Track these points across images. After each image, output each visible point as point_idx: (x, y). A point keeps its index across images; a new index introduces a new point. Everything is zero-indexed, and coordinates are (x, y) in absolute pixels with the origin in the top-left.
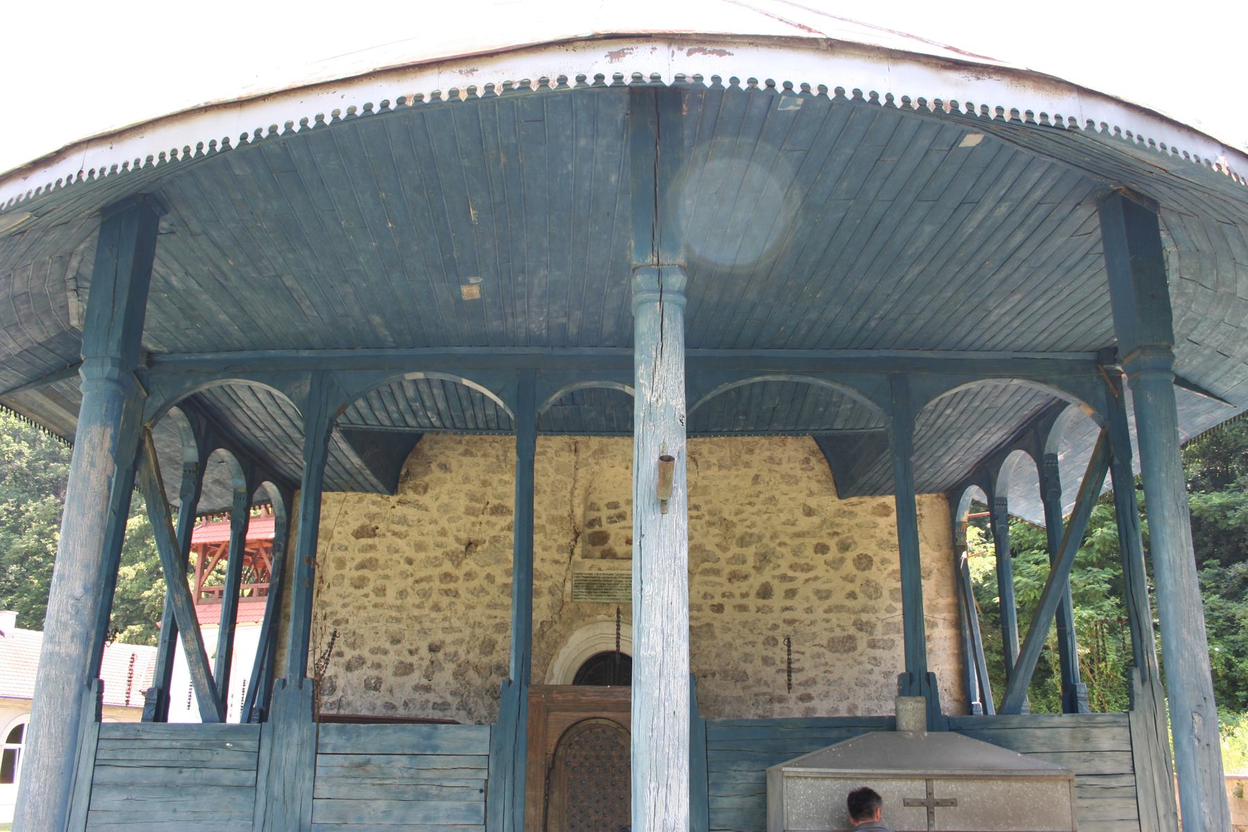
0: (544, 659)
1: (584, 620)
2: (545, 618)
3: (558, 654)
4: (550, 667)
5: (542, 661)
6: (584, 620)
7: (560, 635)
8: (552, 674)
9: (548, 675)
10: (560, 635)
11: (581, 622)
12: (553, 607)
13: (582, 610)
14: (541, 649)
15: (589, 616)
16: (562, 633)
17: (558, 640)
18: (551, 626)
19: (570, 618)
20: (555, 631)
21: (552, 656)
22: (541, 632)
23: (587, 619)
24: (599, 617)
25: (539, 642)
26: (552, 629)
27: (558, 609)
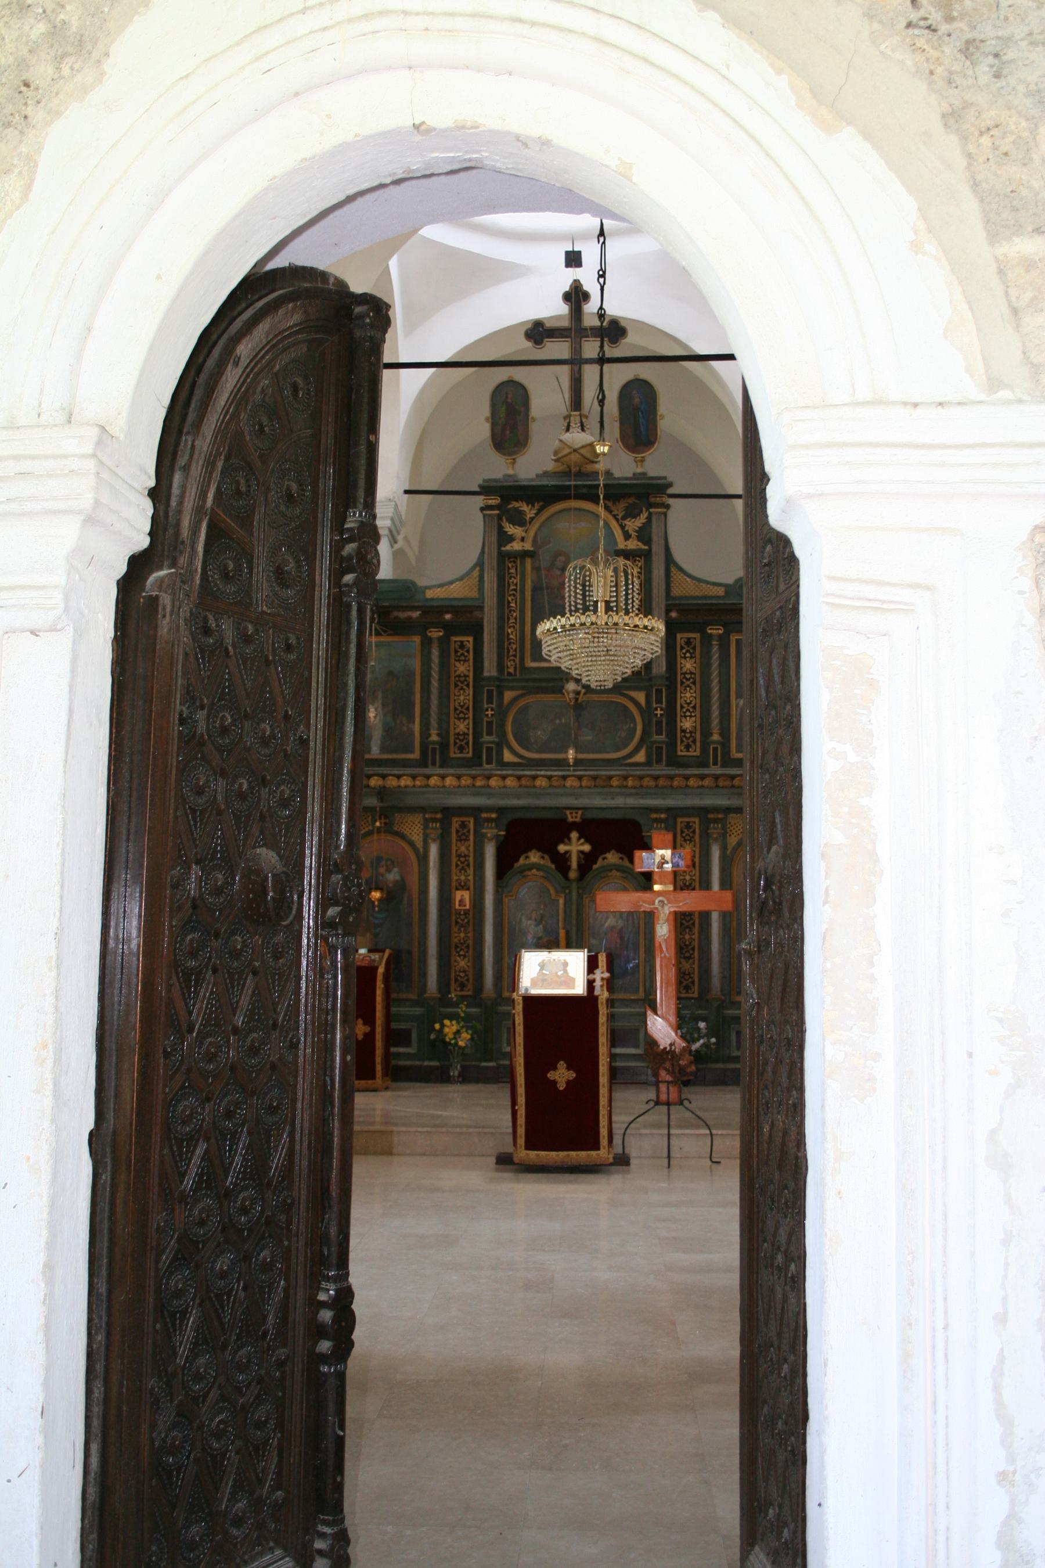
7: (57, 31)
10: (57, 31)
17: (41, 71)
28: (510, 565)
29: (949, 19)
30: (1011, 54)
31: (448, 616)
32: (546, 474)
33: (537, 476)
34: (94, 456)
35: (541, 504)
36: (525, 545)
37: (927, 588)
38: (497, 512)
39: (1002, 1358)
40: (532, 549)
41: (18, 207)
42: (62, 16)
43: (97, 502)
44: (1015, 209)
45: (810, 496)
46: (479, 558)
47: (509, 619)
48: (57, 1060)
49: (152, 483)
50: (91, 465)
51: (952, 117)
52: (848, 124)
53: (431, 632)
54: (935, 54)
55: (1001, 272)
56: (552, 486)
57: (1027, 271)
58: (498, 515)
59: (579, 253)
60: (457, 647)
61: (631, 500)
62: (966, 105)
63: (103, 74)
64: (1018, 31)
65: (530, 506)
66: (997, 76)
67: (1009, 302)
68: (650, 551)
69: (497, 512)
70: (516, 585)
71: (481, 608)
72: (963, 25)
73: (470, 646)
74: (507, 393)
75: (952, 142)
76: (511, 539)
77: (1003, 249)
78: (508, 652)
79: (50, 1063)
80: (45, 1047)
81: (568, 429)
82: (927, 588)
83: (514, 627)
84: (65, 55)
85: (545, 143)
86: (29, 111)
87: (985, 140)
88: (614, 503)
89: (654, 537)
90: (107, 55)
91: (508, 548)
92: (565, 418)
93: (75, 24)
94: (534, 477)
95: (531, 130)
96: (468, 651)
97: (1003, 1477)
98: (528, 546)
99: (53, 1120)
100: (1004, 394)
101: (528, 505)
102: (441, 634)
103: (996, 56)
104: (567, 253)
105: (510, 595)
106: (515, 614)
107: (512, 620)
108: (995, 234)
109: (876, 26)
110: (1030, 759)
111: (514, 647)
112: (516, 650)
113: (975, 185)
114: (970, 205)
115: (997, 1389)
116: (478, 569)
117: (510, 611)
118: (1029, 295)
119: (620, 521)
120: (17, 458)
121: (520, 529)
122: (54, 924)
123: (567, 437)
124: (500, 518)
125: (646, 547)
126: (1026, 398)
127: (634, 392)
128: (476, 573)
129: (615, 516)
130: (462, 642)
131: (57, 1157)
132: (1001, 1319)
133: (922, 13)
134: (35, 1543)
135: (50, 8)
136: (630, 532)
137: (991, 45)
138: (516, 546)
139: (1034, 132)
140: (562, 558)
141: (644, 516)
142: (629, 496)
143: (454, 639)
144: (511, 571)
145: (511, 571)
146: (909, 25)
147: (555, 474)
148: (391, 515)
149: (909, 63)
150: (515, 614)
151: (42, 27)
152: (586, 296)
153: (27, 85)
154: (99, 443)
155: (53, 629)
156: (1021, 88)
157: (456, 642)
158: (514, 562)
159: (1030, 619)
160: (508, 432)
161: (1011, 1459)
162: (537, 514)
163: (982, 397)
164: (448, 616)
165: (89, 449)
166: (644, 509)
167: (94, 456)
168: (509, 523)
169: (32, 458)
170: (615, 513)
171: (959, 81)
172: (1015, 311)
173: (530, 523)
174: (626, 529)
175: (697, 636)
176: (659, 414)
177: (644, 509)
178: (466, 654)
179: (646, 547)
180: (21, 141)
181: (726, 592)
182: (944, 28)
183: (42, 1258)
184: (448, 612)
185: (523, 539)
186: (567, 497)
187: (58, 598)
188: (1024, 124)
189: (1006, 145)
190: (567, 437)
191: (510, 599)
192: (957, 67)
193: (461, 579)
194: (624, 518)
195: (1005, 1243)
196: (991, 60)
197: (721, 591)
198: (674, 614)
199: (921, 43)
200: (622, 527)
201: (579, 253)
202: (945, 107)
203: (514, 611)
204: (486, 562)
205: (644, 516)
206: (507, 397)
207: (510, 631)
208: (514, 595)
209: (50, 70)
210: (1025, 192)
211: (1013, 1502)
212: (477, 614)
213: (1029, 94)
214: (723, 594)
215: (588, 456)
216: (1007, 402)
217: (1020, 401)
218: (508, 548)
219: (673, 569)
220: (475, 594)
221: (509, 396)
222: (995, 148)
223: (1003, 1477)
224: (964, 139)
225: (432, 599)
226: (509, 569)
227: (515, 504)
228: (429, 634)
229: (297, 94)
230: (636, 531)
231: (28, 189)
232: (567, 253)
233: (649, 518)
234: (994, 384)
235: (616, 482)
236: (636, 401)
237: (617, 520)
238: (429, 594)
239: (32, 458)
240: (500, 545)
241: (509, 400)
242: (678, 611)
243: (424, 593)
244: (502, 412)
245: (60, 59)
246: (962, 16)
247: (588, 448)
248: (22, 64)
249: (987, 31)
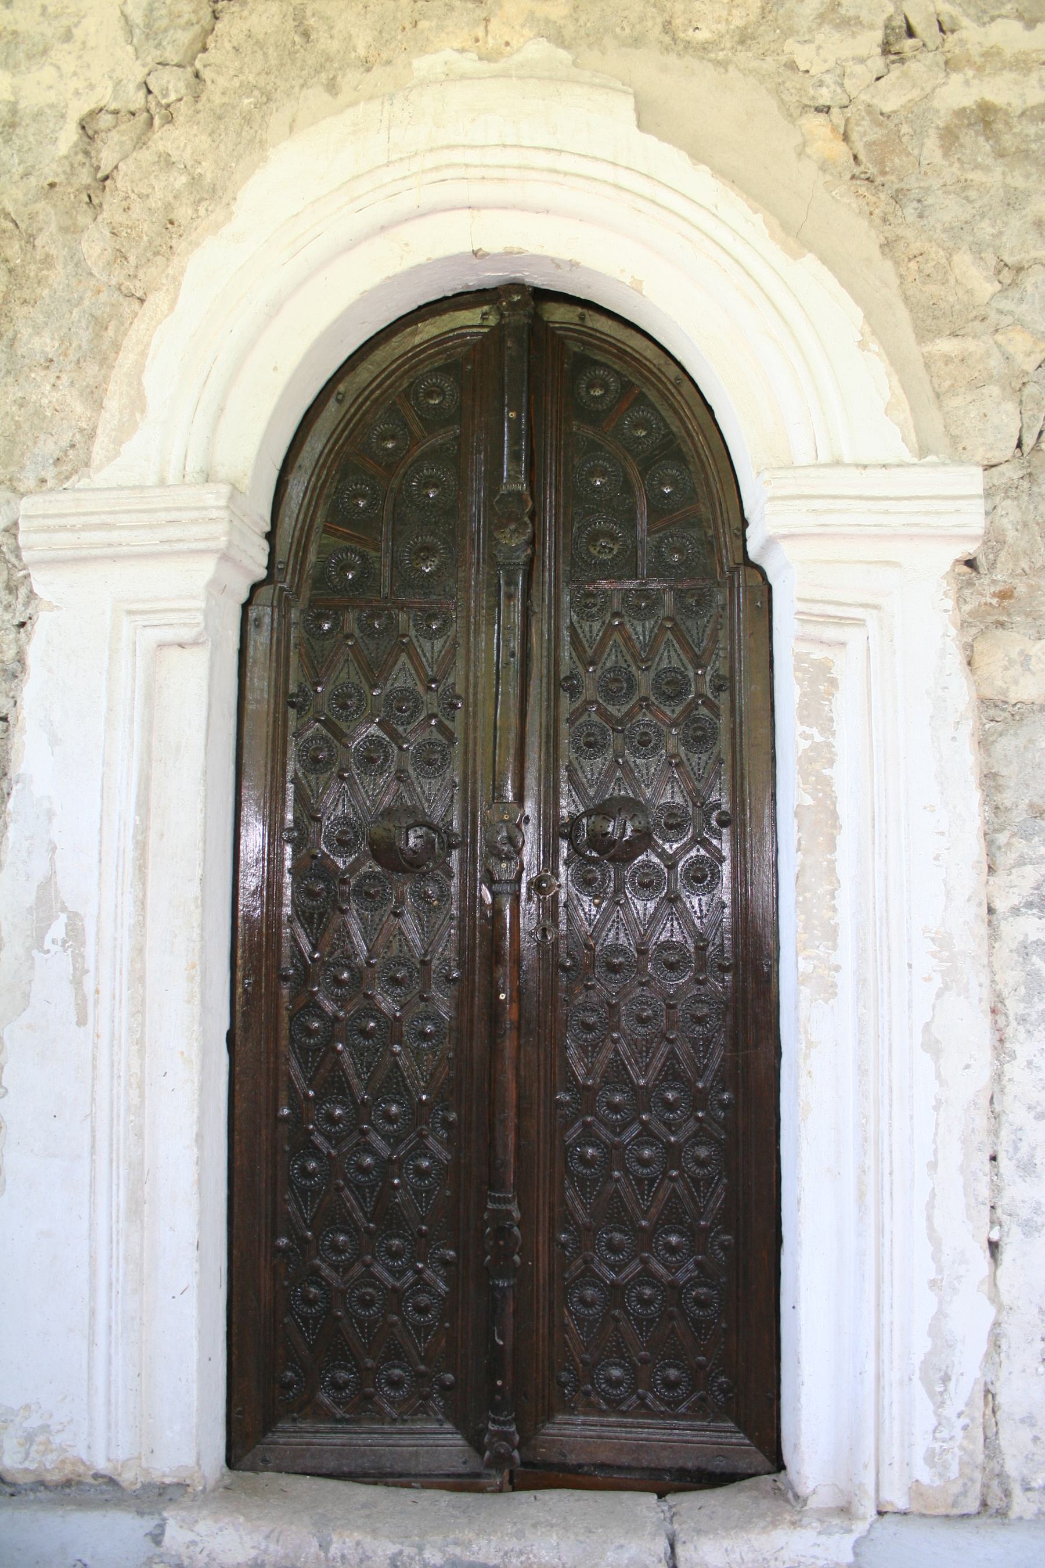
0: (99, 325)
1: (332, 87)
2: (104, 95)
3: (176, 281)
4: (126, 360)
5: (84, 336)
6: (332, 87)
7: (195, 181)
8: (138, 403)
9: (112, 404)
10: (195, 181)
11: (316, 96)
12: (152, 33)
13: (324, 42)
14: (78, 263)
15: (367, 66)
16: (207, 169)
17: (183, 213)
18: (141, 142)
19: (249, 89)
20: (166, 162)
21: (142, 301)
22: (85, 177)
23: (351, 78)
24: (423, 64)
25: (71, 230)
26: (146, 156)
27: (184, 37)
29: (883, 173)
30: (930, 201)
34: (227, 507)
37: (875, 607)
39: (933, 1195)
41: (166, 316)
42: (199, 170)
43: (230, 543)
44: (935, 318)
45: (785, 537)
48: (203, 977)
49: (268, 528)
50: (224, 514)
51: (887, 246)
52: (810, 251)
54: (873, 199)
55: (927, 366)
57: (946, 364)
62: (898, 238)
63: (232, 213)
64: (935, 183)
66: (921, 216)
67: (934, 388)
72: (893, 178)
75: (888, 265)
77: (928, 348)
79: (198, 979)
80: (194, 967)
82: (875, 607)
84: (201, 200)
85: (573, 265)
86: (174, 242)
87: (913, 265)
90: (235, 199)
93: (209, 178)
95: (566, 255)
97: (933, 1284)
99: (201, 1023)
100: (931, 458)
103: (919, 201)
108: (923, 334)
109: (828, 178)
110: (954, 739)
113: (906, 299)
114: (903, 314)
115: (929, 1219)
118: (948, 383)
120: (167, 510)
122: (199, 872)
126: (948, 461)
131: (205, 1052)
132: (933, 1166)
133: (862, 168)
134: (195, 1344)
135: (189, 165)
137: (915, 193)
139: (949, 259)
146: (853, 177)
149: (854, 205)
151: (184, 179)
153: (172, 223)
154: (231, 498)
155: (195, 643)
156: (939, 226)
159: (953, 632)
161: (940, 1270)
163: (915, 460)
165: (223, 502)
167: (227, 507)
169: (179, 509)
171: (890, 218)
172: (938, 396)
180: (168, 266)
182: (879, 180)
183: (195, 1129)
187: (200, 618)
188: (942, 253)
189: (928, 268)
192: (890, 209)
195: (936, 1108)
196: (915, 204)
199: (862, 190)
202: (883, 240)
209: (190, 211)
210: (942, 305)
211: (940, 1303)
213: (945, 231)
216: (934, 465)
217: (944, 464)
222: (920, 271)
223: (933, 1284)
224: (897, 263)
229: (383, 228)
231: (174, 302)
234: (923, 451)
239: (179, 509)
245: (198, 202)
246: (893, 170)
248: (168, 207)
249: (912, 183)
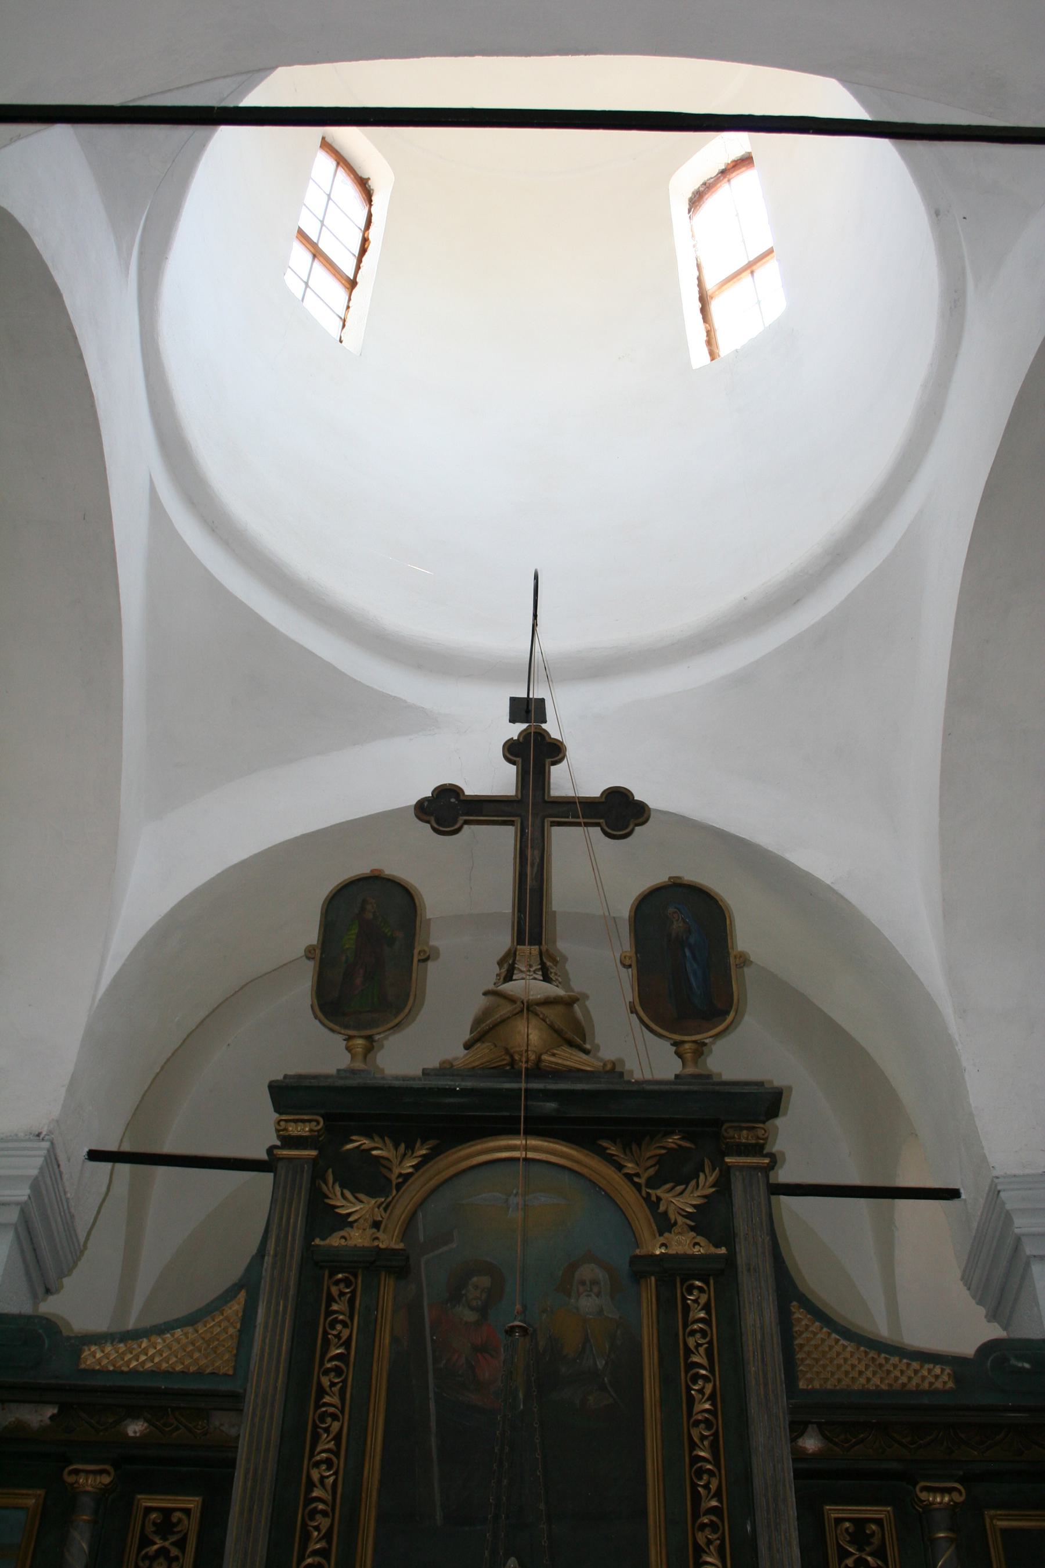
28: (334, 1290)
31: (135, 1428)
32: (446, 1069)
33: (426, 1072)
35: (432, 1143)
36: (380, 1235)
38: (314, 1153)
40: (401, 1246)
46: (248, 1270)
47: (316, 1438)
53: (76, 1472)
56: (465, 1092)
58: (315, 1161)
59: (541, 702)
60: (150, 1528)
61: (673, 1141)
65: (403, 1146)
68: (730, 1260)
69: (314, 1153)
70: (347, 1344)
71: (233, 1401)
73: (191, 1527)
74: (364, 902)
76: (344, 1222)
78: (306, 1537)
81: (509, 977)
83: (329, 1463)
88: (626, 1147)
89: (741, 1226)
91: (335, 1241)
92: (500, 963)
94: (420, 1073)
96: (181, 1544)
98: (388, 1240)
101: (396, 1147)
102: (106, 1480)
104: (514, 701)
105: (327, 1372)
106: (336, 1426)
107: (326, 1443)
111: (325, 1523)
112: (328, 1536)
116: (243, 1294)
117: (322, 1418)
119: (644, 1190)
121: (373, 1201)
123: (508, 987)
124: (318, 1175)
125: (723, 1250)
127: (671, 910)
128: (235, 1307)
129: (629, 1177)
130: (167, 1512)
136: (672, 1216)
138: (357, 1238)
140: (485, 1281)
141: (706, 1183)
142: (668, 1126)
143: (146, 1501)
144: (335, 1307)
145: (335, 1307)
147: (473, 1072)
148: (35, 1172)
150: (336, 1426)
152: (555, 751)
157: (149, 1510)
158: (347, 1282)
160: (359, 980)
162: (416, 1167)
164: (135, 1428)
166: (707, 1162)
168: (342, 1186)
170: (630, 1167)
173: (399, 1187)
174: (662, 1209)
175: (882, 1512)
176: (733, 953)
177: (707, 1162)
178: (175, 1552)
179: (723, 1250)
181: (957, 1378)
184: (133, 1413)
185: (376, 1225)
186: (509, 1128)
190: (508, 987)
191: (325, 1381)
193: (191, 1320)
194: (654, 1182)
197: (942, 1379)
198: (811, 1443)
200: (653, 1204)
201: (541, 702)
203: (335, 1417)
204: (266, 1274)
205: (706, 1183)
206: (363, 909)
207: (315, 1475)
208: (338, 1371)
212: (222, 1422)
214: (950, 1385)
215: (559, 1024)
218: (335, 1241)
219: (798, 1314)
220: (223, 1364)
221: (369, 907)
225: (93, 1372)
226: (331, 1299)
227: (360, 1142)
228: (70, 1479)
230: (688, 1216)
232: (514, 701)
233: (724, 1186)
235: (635, 1088)
236: (677, 926)
237: (638, 1187)
238: (94, 1357)
240: (308, 1237)
241: (369, 916)
242: (823, 1430)
243: (77, 1353)
244: (350, 940)
247: (560, 1009)
